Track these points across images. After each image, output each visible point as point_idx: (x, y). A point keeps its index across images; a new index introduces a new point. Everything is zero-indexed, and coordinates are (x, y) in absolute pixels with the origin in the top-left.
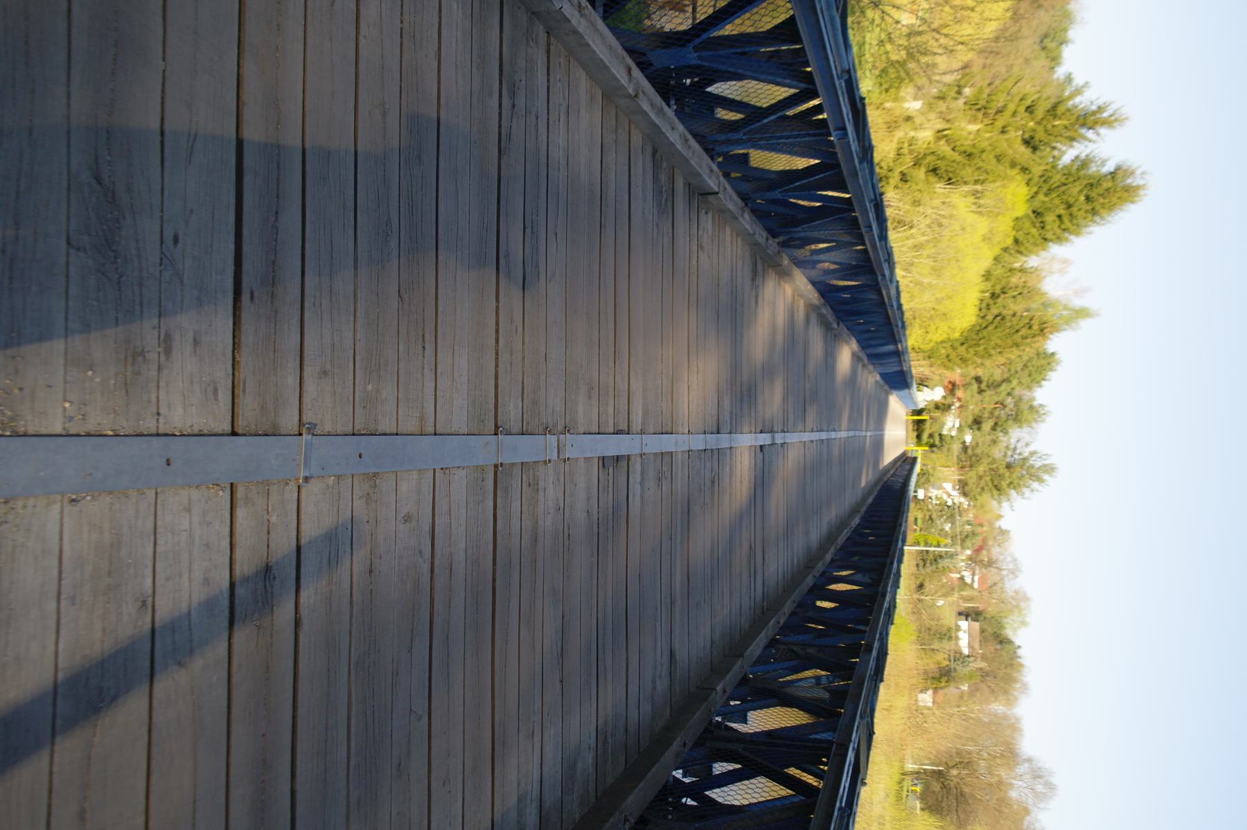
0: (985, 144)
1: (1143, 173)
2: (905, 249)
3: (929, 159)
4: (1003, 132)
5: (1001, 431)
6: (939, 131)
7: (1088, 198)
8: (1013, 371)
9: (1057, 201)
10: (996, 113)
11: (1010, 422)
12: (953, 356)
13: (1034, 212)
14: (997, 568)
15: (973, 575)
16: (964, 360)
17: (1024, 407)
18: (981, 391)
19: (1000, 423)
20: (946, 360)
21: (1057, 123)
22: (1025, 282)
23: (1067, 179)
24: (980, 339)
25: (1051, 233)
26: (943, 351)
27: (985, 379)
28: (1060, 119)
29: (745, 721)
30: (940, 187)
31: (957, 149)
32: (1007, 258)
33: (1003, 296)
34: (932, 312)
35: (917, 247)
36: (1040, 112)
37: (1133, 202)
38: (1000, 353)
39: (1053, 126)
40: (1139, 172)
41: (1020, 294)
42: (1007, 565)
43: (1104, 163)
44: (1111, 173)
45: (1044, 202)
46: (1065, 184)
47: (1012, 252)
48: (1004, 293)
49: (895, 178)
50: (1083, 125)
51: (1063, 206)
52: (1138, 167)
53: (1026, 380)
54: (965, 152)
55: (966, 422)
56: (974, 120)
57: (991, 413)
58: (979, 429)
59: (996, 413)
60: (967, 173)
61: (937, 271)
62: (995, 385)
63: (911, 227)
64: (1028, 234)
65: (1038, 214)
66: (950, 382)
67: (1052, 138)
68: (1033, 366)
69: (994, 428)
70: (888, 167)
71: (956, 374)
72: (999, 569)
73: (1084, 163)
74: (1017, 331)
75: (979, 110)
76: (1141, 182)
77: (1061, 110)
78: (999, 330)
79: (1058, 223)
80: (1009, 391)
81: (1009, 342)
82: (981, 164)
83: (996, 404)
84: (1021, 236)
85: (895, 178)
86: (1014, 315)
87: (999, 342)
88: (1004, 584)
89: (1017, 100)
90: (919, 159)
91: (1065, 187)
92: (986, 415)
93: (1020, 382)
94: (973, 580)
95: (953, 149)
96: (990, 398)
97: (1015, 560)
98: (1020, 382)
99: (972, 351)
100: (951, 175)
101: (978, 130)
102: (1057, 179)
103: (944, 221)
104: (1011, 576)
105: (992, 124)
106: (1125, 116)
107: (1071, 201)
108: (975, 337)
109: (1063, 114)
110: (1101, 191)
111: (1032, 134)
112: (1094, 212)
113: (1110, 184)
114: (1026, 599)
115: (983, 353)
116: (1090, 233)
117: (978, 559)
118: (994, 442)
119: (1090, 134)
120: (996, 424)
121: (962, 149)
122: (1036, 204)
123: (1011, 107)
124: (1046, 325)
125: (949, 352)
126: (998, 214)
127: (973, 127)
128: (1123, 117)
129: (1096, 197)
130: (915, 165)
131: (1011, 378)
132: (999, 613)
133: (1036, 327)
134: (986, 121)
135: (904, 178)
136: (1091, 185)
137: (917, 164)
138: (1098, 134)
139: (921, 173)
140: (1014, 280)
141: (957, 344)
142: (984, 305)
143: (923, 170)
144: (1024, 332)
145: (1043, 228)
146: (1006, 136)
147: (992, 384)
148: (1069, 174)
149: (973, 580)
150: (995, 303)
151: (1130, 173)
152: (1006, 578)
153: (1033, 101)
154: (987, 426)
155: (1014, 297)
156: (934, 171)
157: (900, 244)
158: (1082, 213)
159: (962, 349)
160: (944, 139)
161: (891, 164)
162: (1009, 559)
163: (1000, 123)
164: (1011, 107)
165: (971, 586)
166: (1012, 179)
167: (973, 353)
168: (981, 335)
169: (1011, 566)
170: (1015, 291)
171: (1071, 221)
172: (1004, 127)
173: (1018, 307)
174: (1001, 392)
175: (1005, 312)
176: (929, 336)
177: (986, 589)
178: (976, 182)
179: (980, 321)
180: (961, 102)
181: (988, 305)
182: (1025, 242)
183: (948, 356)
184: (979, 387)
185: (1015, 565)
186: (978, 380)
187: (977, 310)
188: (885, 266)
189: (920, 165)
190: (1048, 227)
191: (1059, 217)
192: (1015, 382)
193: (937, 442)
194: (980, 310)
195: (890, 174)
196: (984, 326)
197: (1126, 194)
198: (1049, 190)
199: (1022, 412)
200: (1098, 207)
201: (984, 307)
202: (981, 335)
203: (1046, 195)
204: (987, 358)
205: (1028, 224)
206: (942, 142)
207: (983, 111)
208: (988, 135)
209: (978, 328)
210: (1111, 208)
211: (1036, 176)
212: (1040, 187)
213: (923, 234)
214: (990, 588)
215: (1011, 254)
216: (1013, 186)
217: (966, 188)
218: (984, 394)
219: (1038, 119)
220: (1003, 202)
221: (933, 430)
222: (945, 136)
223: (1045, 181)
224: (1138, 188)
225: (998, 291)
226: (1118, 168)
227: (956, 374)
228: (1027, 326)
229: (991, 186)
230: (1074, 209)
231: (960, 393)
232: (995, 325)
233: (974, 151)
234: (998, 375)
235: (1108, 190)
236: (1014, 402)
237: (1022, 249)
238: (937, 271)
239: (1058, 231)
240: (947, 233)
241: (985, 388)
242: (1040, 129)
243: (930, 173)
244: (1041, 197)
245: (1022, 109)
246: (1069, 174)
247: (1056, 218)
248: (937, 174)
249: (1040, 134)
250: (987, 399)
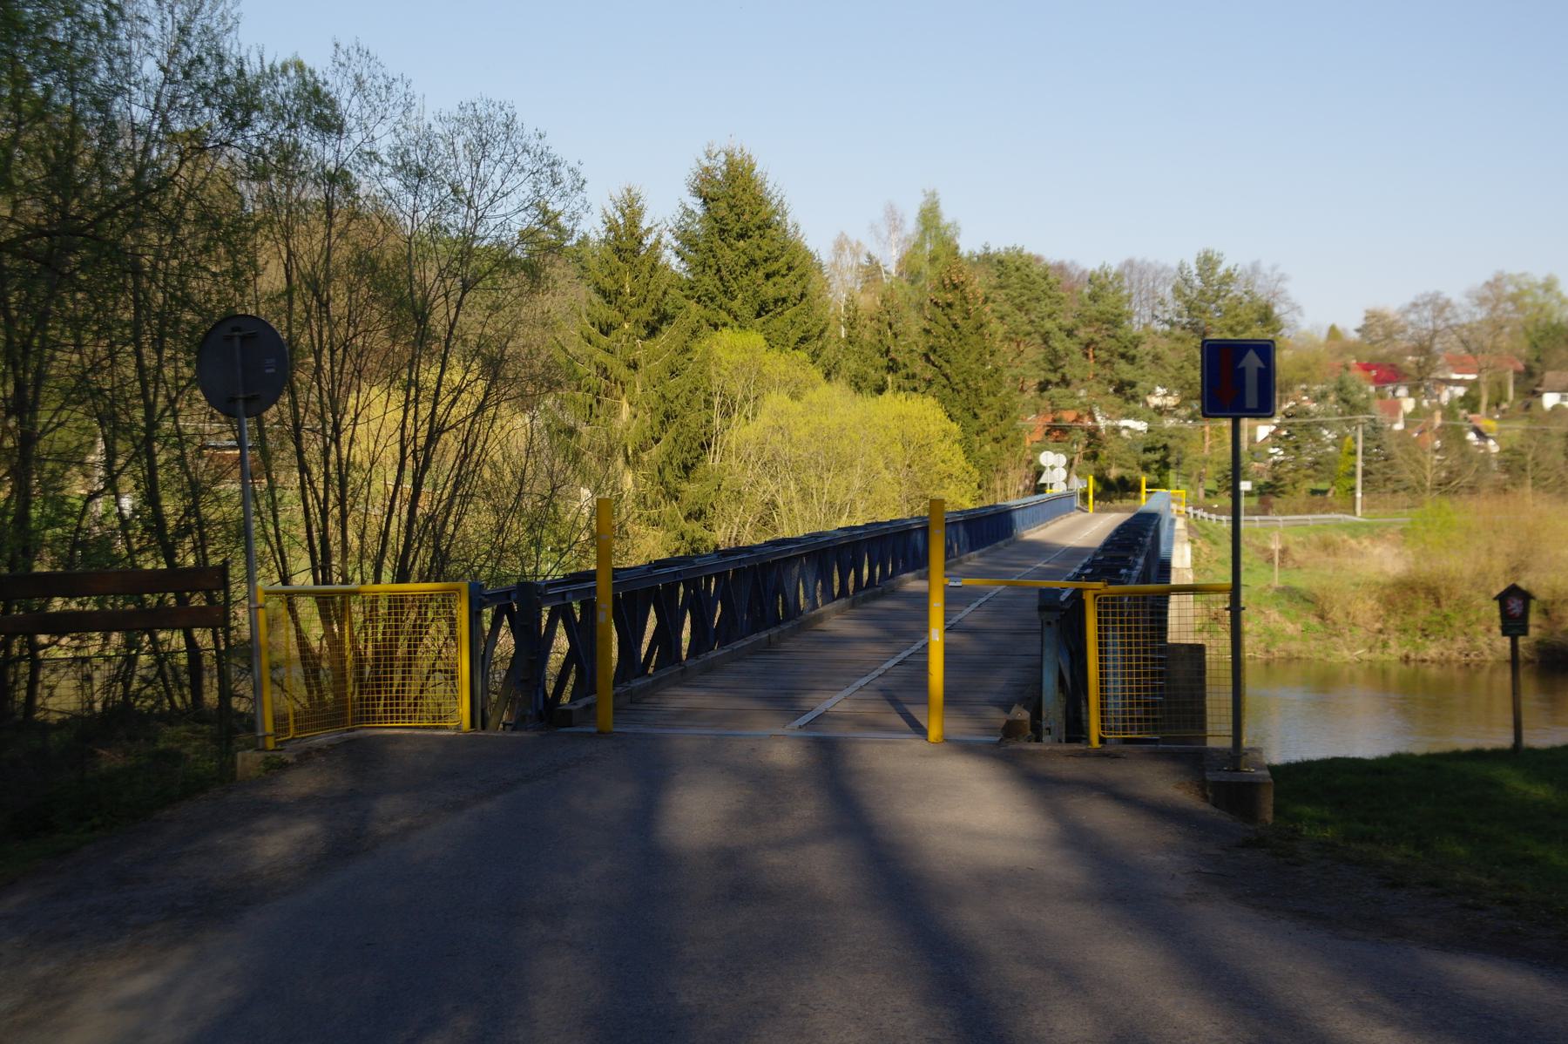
0: (654, 397)
1: (708, 157)
2: (807, 515)
3: (669, 476)
4: (634, 366)
5: (1136, 347)
6: (627, 462)
7: (742, 236)
8: (1029, 328)
9: (745, 281)
10: (607, 378)
11: (1120, 332)
12: (995, 431)
13: (759, 315)
14: (1432, 339)
15: (1448, 382)
16: (1004, 414)
17: (1093, 310)
18: (1065, 382)
19: (1122, 350)
20: (1003, 443)
21: (628, 291)
22: (872, 319)
23: (710, 267)
24: (968, 387)
25: (793, 289)
26: (988, 448)
27: (1043, 376)
28: (623, 286)
29: (1196, 652)
30: (712, 461)
31: (656, 435)
32: (828, 353)
33: (893, 355)
34: (915, 468)
35: (805, 494)
36: (609, 313)
37: (751, 168)
38: (992, 354)
39: (632, 295)
40: (706, 163)
41: (890, 326)
42: (1424, 321)
43: (689, 213)
44: (705, 202)
45: (745, 301)
46: (719, 270)
47: (820, 344)
48: (888, 351)
49: (695, 528)
50: (636, 253)
51: (752, 272)
52: (699, 161)
53: (1045, 307)
54: (662, 423)
55: (1120, 408)
56: (614, 411)
57: (1104, 364)
58: (1132, 385)
59: (1104, 355)
60: (694, 419)
61: (843, 465)
62: (1054, 361)
63: (775, 506)
64: (793, 323)
65: (762, 308)
66: (1048, 433)
67: (650, 296)
68: (1021, 295)
69: (1131, 360)
70: (677, 539)
71: (1033, 424)
72: (1435, 333)
73: (687, 240)
74: (955, 326)
75: (598, 402)
76: (722, 158)
77: (608, 284)
78: (952, 358)
79: (777, 279)
80: (1063, 335)
81: (974, 339)
82: (683, 401)
83: (1087, 355)
84: (794, 335)
85: (695, 528)
86: (927, 332)
87: (974, 356)
88: (1463, 326)
89: (590, 348)
90: (668, 493)
91: (724, 272)
92: (1106, 372)
93: (1049, 316)
94: (1459, 383)
95: (657, 441)
96: (1076, 366)
97: (1415, 305)
98: (1049, 316)
99: (987, 401)
100: (696, 445)
101: (630, 404)
102: (709, 281)
103: (767, 455)
104: (1447, 314)
105: (622, 383)
106: (625, 193)
107: (744, 259)
108: (964, 396)
109: (616, 282)
110: (731, 218)
111: (641, 325)
112: (765, 226)
113: (723, 205)
114: (1495, 284)
115: (992, 382)
116: (796, 226)
117: (1414, 373)
118: (1157, 358)
119: (649, 241)
120: (1123, 356)
121: (657, 428)
122: (747, 312)
123: (600, 356)
124: (947, 282)
125: (990, 439)
126: (759, 372)
127: (626, 411)
128: (627, 197)
129: (740, 225)
130: (677, 499)
131: (1043, 331)
132: (1528, 334)
133: (950, 297)
134: (617, 392)
135: (696, 515)
136: (722, 231)
137: (674, 496)
138: (650, 230)
139: (690, 489)
140: (867, 336)
141: (976, 425)
142: (907, 384)
143: (685, 486)
144: (957, 317)
145: (784, 300)
146: (643, 362)
147: (1051, 362)
148: (704, 264)
149: (1459, 383)
150: (905, 365)
151: (706, 176)
152: (1452, 322)
153: (593, 324)
154: (1125, 371)
155: (895, 335)
156: (687, 468)
157: (799, 521)
158: (763, 244)
159: (985, 416)
160: (641, 454)
161: (673, 534)
162: (1412, 317)
163: (624, 373)
164: (600, 356)
165: (1474, 385)
166: (708, 352)
167: (992, 399)
168: (961, 386)
169: (1427, 313)
170: (885, 334)
171: (777, 259)
172: (629, 366)
173: (913, 324)
174: (1066, 349)
175: (921, 349)
176: (956, 471)
177: (1475, 357)
178: (708, 404)
179: (934, 389)
180: (584, 429)
181: (908, 377)
182: (805, 328)
183: (996, 440)
184: (1057, 384)
185: (1425, 304)
186: (1043, 387)
187: (914, 395)
188: (821, 540)
189: (677, 490)
190: (784, 293)
191: (768, 276)
192: (1049, 325)
193: (1157, 456)
194: (915, 390)
195: (688, 537)
196: (945, 382)
197: (740, 182)
198: (725, 292)
199: (1102, 313)
200: (757, 220)
201: (912, 385)
202: (961, 386)
203: (734, 298)
204: (1001, 375)
205: (777, 323)
206: (645, 457)
207: (602, 397)
208: (638, 390)
209: (948, 391)
210: (761, 201)
211: (704, 312)
212: (720, 307)
213: (786, 488)
214: (1472, 347)
215: (823, 347)
216: (718, 351)
217: (717, 421)
218: (1068, 377)
219: (620, 316)
220: (742, 365)
221: (1133, 463)
222: (635, 453)
223: (712, 300)
224: (730, 163)
225: (884, 361)
226: (698, 192)
227: (1033, 424)
228: (948, 310)
229: (717, 381)
230: (758, 255)
231: (1068, 417)
232: (944, 364)
233: (662, 409)
234: (1034, 353)
235: (731, 207)
236: (1086, 326)
237: (816, 331)
238: (843, 465)
239: (792, 276)
240: (787, 451)
241: (1059, 375)
242: (636, 313)
243: (691, 476)
244: (735, 305)
245: (604, 340)
246: (704, 264)
247: (770, 283)
248: (693, 465)
249: (644, 313)
250: (1078, 372)
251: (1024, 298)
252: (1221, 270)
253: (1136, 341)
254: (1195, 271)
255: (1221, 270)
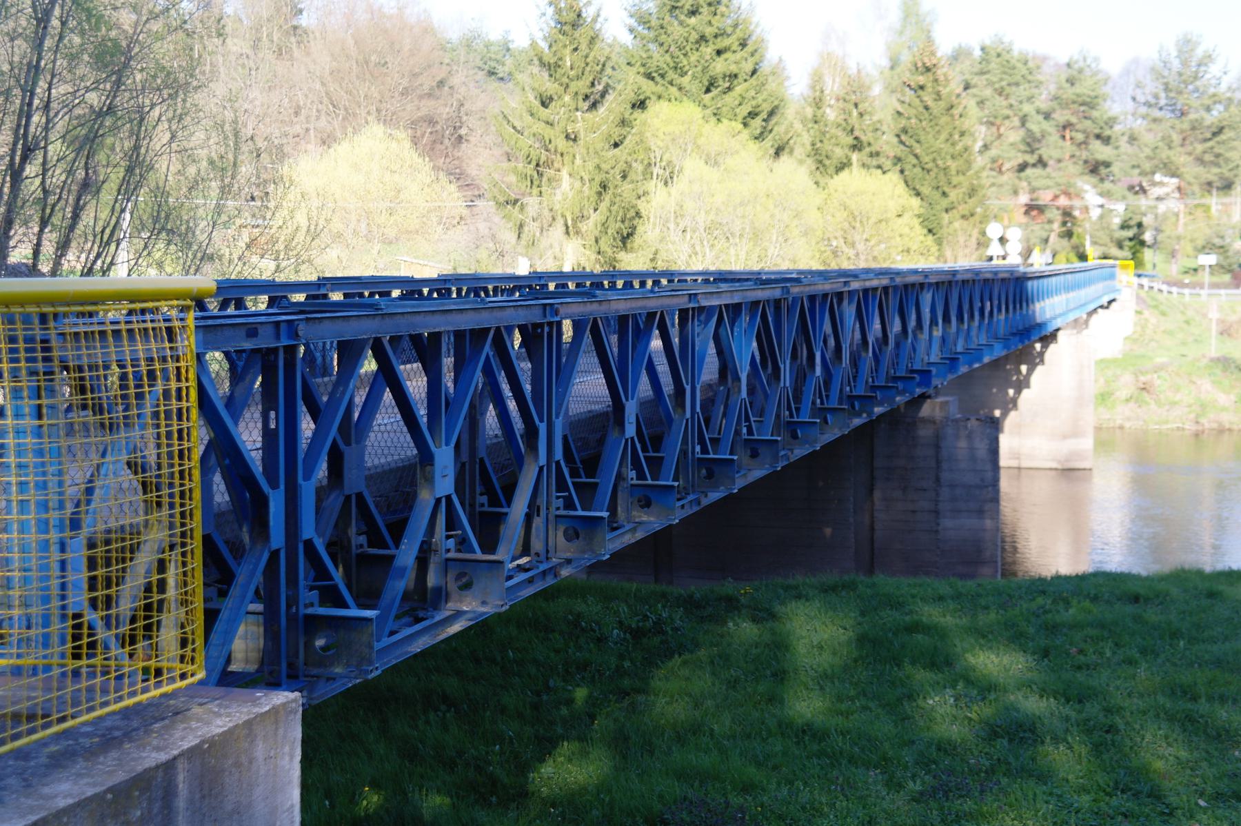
5: (1111, 127)
11: (1095, 114)
12: (963, 209)
16: (972, 192)
17: (1070, 93)
18: (1041, 163)
19: (1097, 131)
21: (569, 64)
24: (937, 166)
27: (1021, 158)
33: (857, 133)
41: (856, 105)
45: (694, 77)
53: (1023, 91)
54: (600, 194)
58: (1107, 165)
62: (1031, 143)
69: (1106, 140)
74: (927, 108)
78: (922, 138)
80: (1040, 118)
81: (944, 120)
83: (1063, 137)
87: (943, 136)
96: (1053, 148)
99: (955, 180)
107: (694, 36)
118: (1133, 139)
120: (1098, 137)
124: (920, 64)
125: (958, 216)
133: (921, 79)
141: (945, 203)
144: (928, 99)
147: (1028, 144)
150: (869, 144)
154: (1101, 151)
155: (861, 115)
159: (953, 195)
167: (961, 178)
170: (850, 114)
181: (871, 155)
183: (963, 217)
184: (1034, 165)
192: (1027, 108)
193: (1130, 233)
196: (915, 161)
199: (1078, 95)
201: (875, 162)
203: (683, 74)
218: (1045, 157)
221: (1106, 240)
223: (662, 76)
225: (850, 140)
228: (920, 92)
231: (1045, 197)
233: (598, 179)
241: (1036, 157)
242: (574, 86)
243: (629, 246)
244: (685, 81)
249: (582, 86)
251: (1004, 83)
252: (1199, 52)
253: (1110, 123)
254: (1174, 53)
255: (1199, 52)
